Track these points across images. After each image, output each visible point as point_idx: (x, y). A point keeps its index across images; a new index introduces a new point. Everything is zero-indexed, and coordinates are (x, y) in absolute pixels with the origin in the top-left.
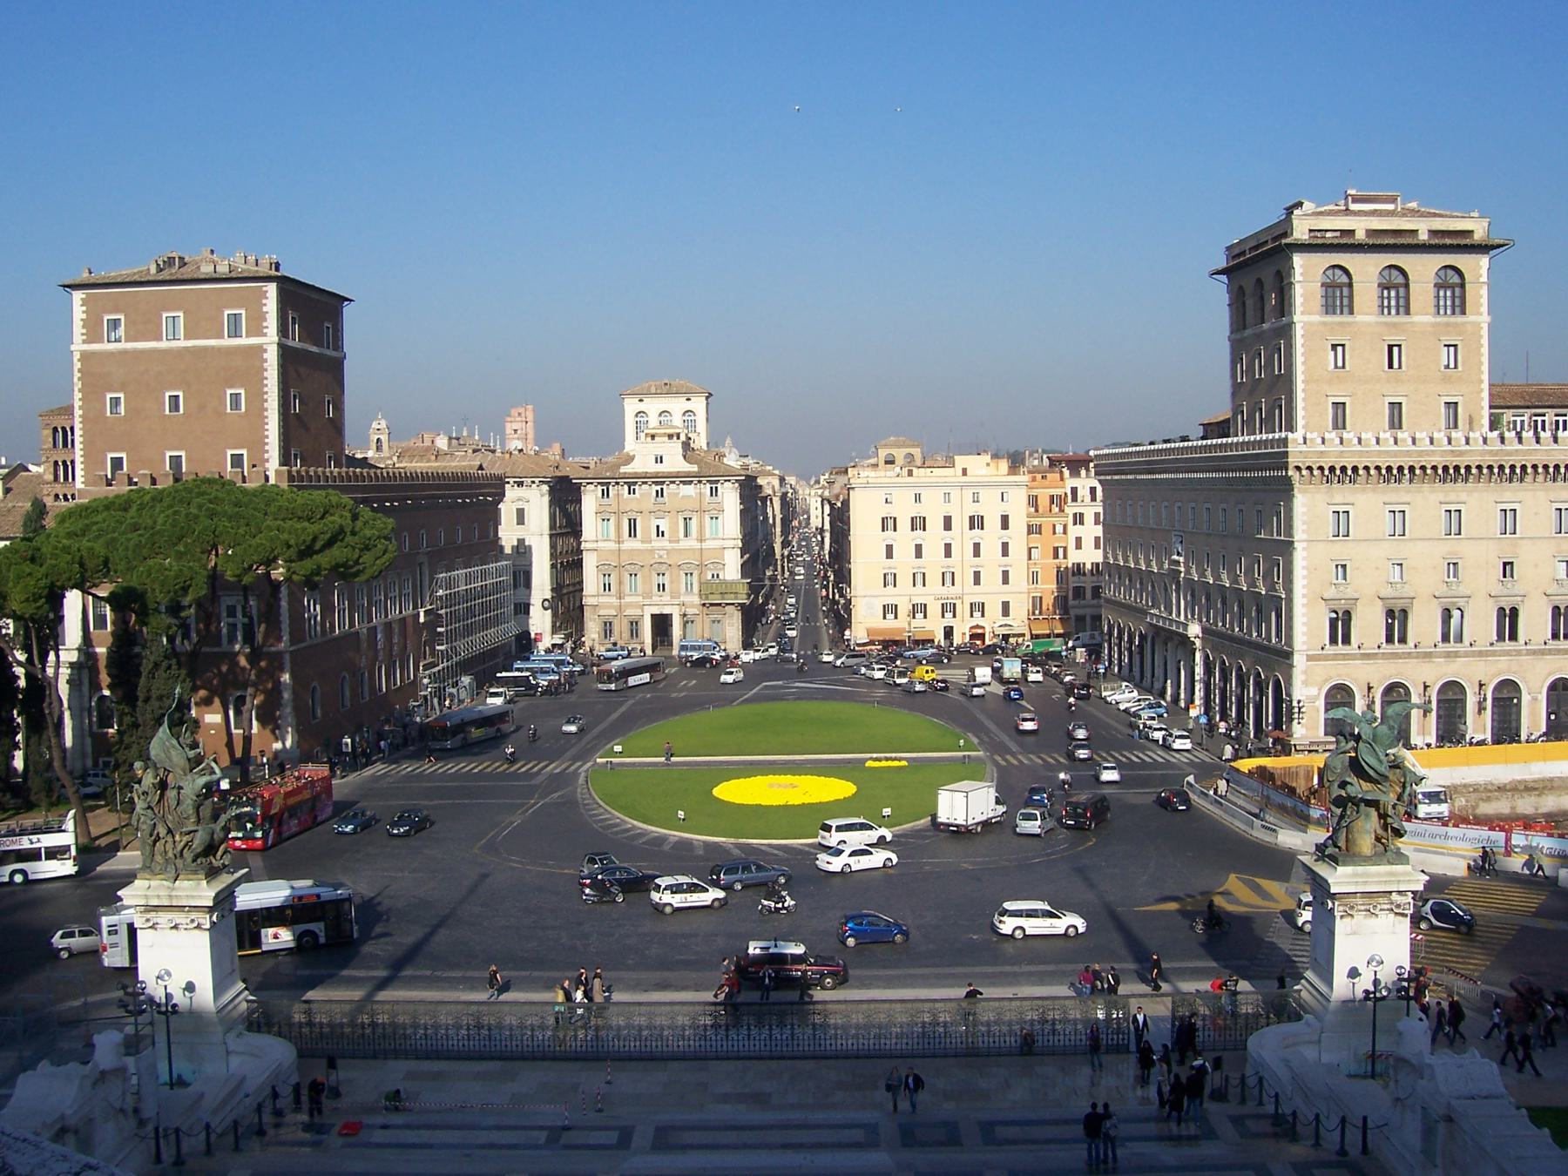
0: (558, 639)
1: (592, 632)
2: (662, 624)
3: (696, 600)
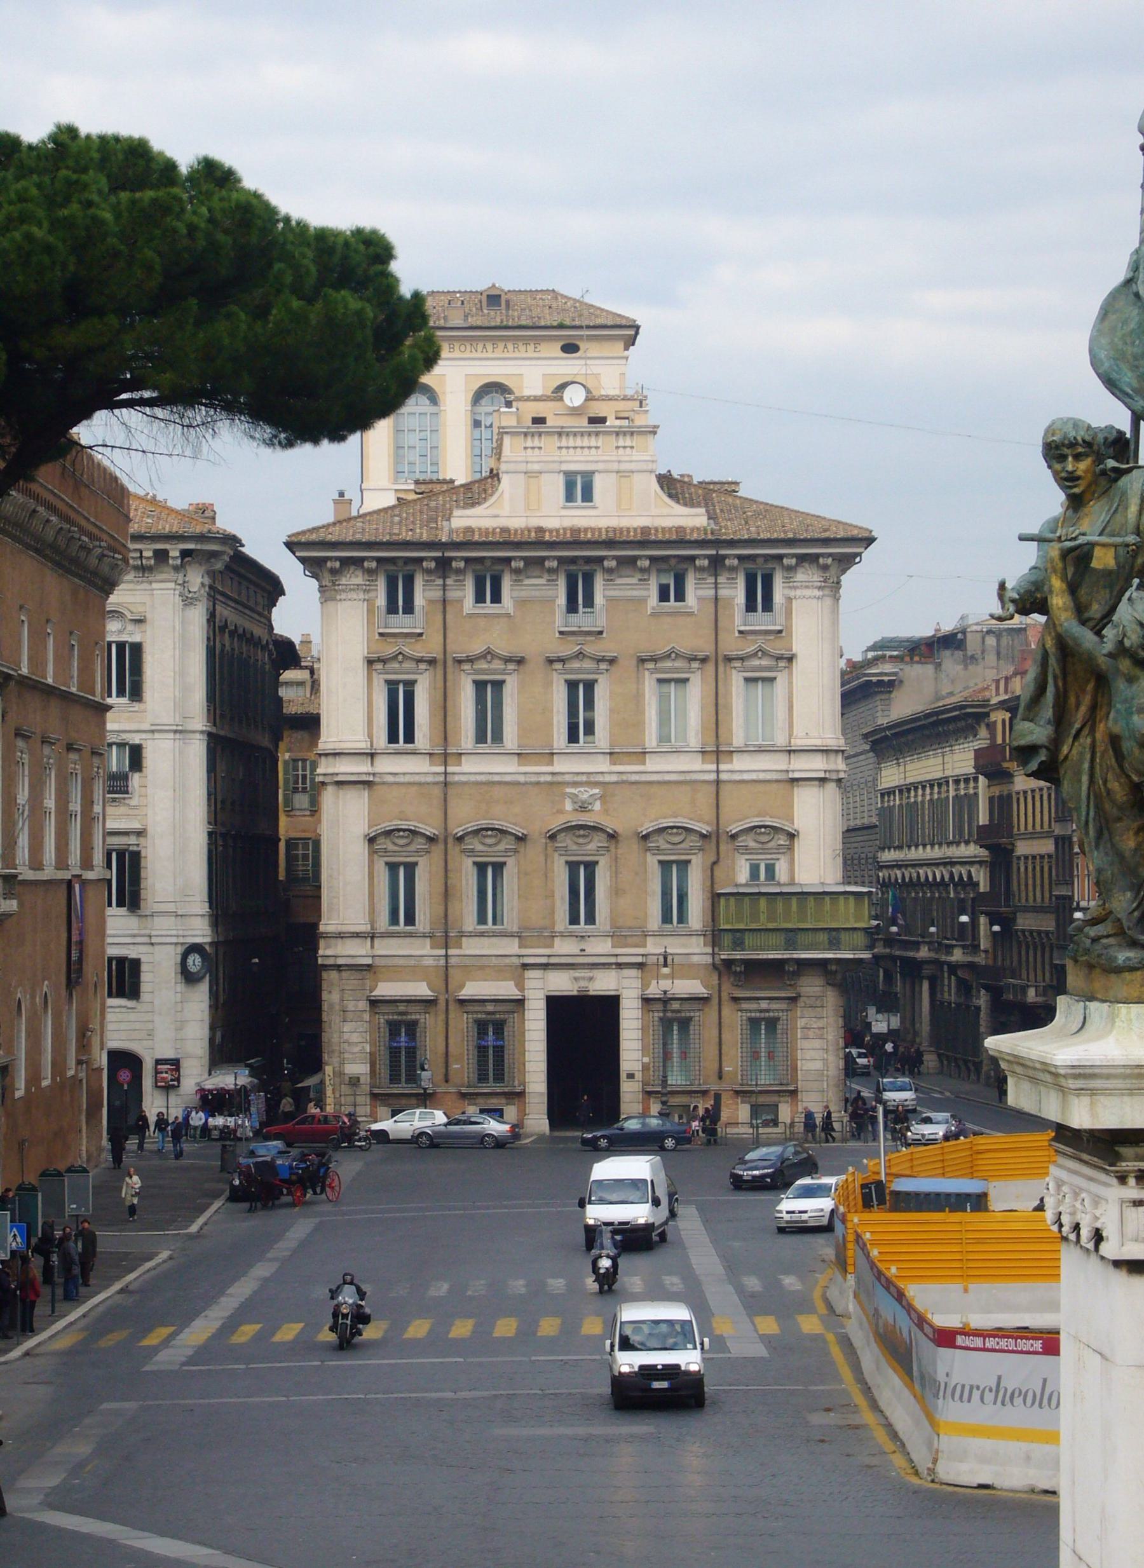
0: (228, 1079)
1: (351, 1046)
2: (584, 1029)
3: (696, 950)
